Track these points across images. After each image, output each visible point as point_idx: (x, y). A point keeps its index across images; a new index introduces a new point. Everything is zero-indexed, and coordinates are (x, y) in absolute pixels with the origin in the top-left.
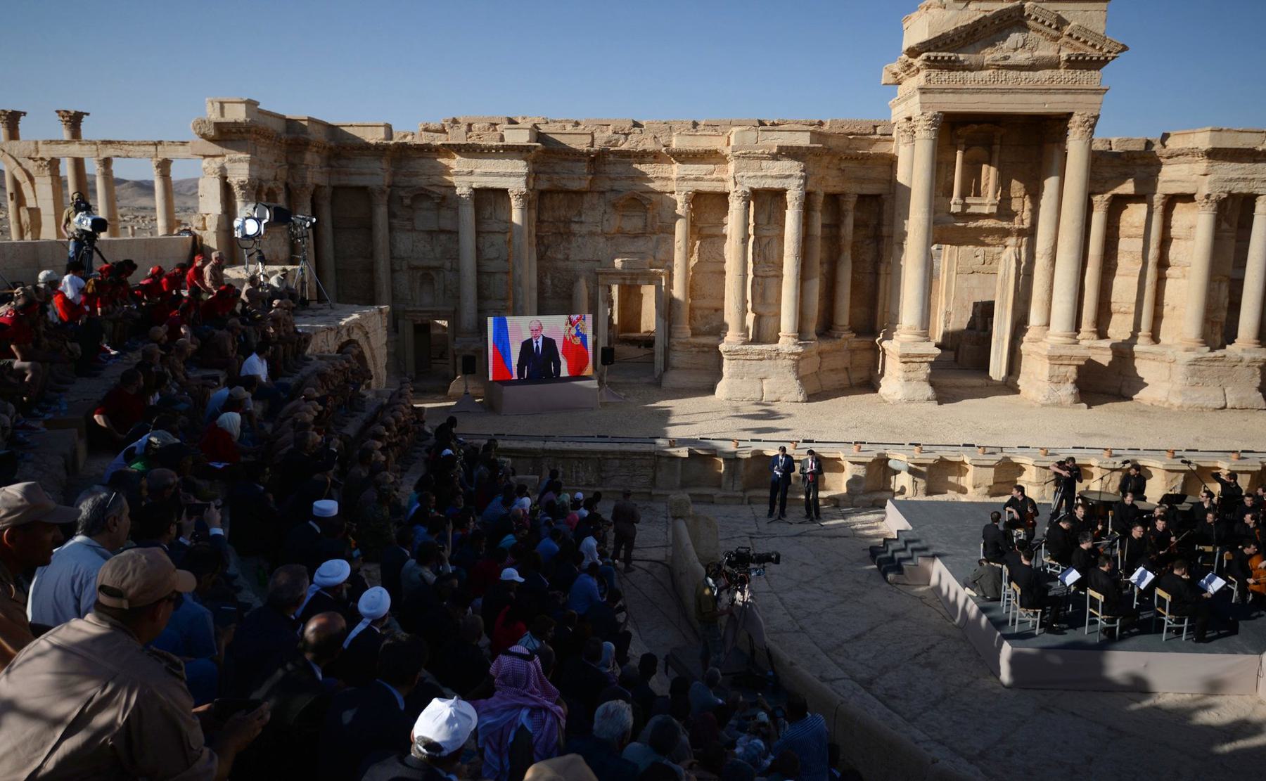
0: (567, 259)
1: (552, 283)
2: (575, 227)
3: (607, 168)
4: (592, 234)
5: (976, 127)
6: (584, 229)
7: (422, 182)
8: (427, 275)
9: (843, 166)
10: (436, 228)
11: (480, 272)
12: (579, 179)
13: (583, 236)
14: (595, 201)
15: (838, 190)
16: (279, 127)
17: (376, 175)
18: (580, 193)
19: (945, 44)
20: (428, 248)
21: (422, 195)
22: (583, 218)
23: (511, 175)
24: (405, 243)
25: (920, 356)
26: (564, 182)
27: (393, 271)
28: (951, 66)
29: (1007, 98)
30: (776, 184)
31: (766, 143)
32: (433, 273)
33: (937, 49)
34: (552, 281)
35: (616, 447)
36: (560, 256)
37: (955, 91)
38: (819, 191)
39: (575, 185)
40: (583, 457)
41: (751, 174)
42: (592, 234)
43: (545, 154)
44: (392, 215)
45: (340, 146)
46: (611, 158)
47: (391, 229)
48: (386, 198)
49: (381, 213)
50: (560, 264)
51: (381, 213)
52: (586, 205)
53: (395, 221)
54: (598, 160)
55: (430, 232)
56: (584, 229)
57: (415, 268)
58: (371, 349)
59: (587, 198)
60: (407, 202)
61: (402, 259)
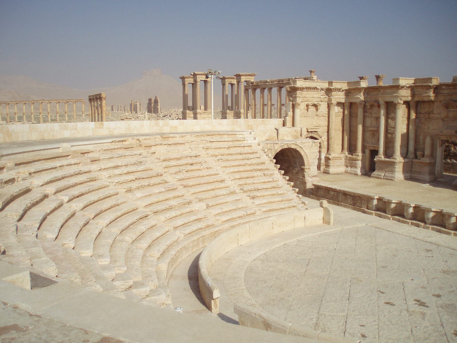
3: (442, 91)
44: (365, 112)
48: (362, 106)
49: (360, 112)
53: (366, 114)
58: (304, 152)
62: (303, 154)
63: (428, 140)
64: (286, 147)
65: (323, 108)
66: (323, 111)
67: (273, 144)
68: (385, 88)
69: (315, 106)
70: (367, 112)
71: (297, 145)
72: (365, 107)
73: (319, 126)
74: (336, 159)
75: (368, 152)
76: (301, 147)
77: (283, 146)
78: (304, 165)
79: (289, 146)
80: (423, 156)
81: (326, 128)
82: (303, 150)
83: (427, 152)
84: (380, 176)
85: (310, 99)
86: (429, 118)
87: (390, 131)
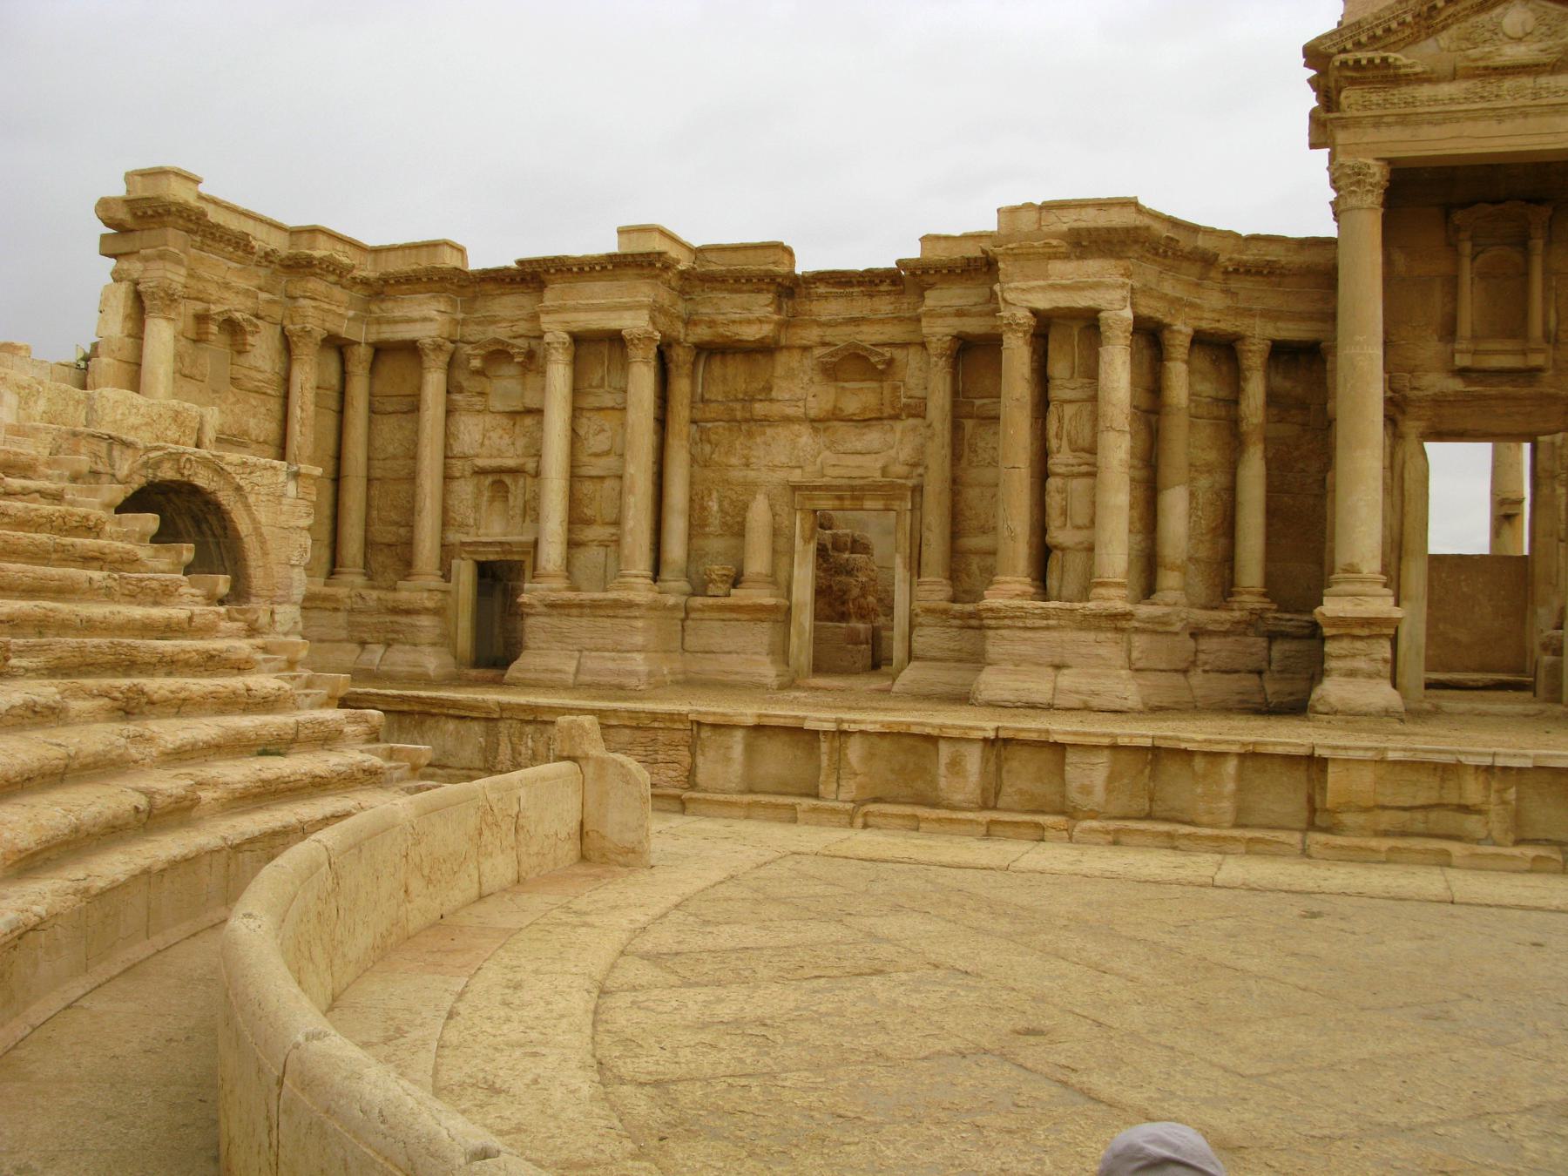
1: (721, 510)
4: (788, 420)
8: (499, 480)
10: (519, 408)
11: (575, 476)
14: (795, 364)
15: (1227, 326)
18: (765, 350)
19: (1374, 38)
20: (507, 440)
22: (774, 394)
23: (627, 307)
24: (473, 433)
26: (735, 329)
27: (447, 478)
28: (1389, 76)
29: (1508, 126)
31: (1053, 228)
32: (508, 480)
33: (1358, 45)
34: (720, 503)
36: (734, 461)
37: (1403, 120)
39: (751, 333)
42: (788, 420)
44: (452, 388)
46: (822, 289)
47: (449, 412)
49: (434, 382)
50: (736, 475)
51: (434, 382)
52: (779, 371)
53: (457, 397)
57: (481, 472)
59: (782, 358)
60: (476, 363)
61: (465, 457)
62: (243, 526)
64: (167, 473)
65: (263, 352)
66: (260, 363)
67: (104, 445)
68: (581, 270)
69: (232, 328)
70: (460, 390)
71: (220, 471)
72: (451, 365)
74: (318, 603)
75: (465, 573)
76: (239, 489)
77: (158, 464)
79: (186, 472)
82: (247, 507)
84: (557, 675)
87: (584, 471)
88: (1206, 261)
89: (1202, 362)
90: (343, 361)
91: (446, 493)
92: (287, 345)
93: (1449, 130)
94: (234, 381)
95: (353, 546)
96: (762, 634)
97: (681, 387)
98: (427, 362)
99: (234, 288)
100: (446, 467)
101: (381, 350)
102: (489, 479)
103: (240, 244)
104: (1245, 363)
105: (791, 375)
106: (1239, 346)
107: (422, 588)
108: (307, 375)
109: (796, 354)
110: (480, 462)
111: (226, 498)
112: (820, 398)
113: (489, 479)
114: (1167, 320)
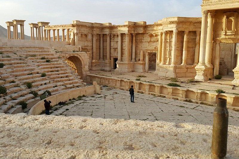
0: (142, 47)
2: (143, 41)
5: (229, 13)
6: (144, 41)
7: (114, 33)
9: (195, 25)
12: (141, 31)
13: (144, 42)
15: (194, 30)
16: (90, 25)
17: (107, 32)
18: (143, 34)
21: (114, 35)
22: (144, 39)
25: (200, 69)
27: (110, 49)
30: (171, 30)
35: (109, 77)
36: (140, 46)
38: (186, 31)
39: (141, 32)
40: (106, 79)
41: (166, 28)
42: (146, 42)
43: (134, 26)
44: (110, 39)
45: (102, 27)
46: (149, 26)
47: (110, 42)
49: (108, 38)
50: (140, 48)
52: (145, 36)
53: (111, 40)
54: (145, 27)
55: (117, 42)
56: (144, 41)
57: (113, 48)
59: (145, 34)
63: (142, 53)
65: (90, 37)
69: (86, 35)
72: (110, 36)
73: (87, 46)
75: (112, 59)
76: (80, 56)
78: (82, 65)
80: (139, 60)
81: (91, 47)
83: (141, 58)
85: (83, 32)
86: (142, 42)
88: (191, 22)
89: (192, 34)
90: (100, 36)
91: (110, 50)
92: (92, 36)
93: (215, 6)
94: (87, 40)
95: (102, 56)
96: (141, 66)
97: (134, 38)
98: (108, 36)
99: (85, 31)
100: (110, 48)
101: (104, 35)
102: (114, 49)
103: (86, 26)
104: (197, 34)
105: (146, 37)
106: (196, 32)
107: (107, 61)
108: (94, 39)
109: (146, 34)
110: (113, 47)
111: (79, 57)
112: (149, 39)
113: (114, 49)
114: (184, 30)
